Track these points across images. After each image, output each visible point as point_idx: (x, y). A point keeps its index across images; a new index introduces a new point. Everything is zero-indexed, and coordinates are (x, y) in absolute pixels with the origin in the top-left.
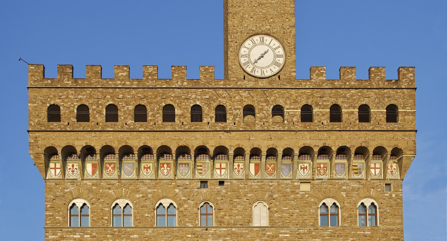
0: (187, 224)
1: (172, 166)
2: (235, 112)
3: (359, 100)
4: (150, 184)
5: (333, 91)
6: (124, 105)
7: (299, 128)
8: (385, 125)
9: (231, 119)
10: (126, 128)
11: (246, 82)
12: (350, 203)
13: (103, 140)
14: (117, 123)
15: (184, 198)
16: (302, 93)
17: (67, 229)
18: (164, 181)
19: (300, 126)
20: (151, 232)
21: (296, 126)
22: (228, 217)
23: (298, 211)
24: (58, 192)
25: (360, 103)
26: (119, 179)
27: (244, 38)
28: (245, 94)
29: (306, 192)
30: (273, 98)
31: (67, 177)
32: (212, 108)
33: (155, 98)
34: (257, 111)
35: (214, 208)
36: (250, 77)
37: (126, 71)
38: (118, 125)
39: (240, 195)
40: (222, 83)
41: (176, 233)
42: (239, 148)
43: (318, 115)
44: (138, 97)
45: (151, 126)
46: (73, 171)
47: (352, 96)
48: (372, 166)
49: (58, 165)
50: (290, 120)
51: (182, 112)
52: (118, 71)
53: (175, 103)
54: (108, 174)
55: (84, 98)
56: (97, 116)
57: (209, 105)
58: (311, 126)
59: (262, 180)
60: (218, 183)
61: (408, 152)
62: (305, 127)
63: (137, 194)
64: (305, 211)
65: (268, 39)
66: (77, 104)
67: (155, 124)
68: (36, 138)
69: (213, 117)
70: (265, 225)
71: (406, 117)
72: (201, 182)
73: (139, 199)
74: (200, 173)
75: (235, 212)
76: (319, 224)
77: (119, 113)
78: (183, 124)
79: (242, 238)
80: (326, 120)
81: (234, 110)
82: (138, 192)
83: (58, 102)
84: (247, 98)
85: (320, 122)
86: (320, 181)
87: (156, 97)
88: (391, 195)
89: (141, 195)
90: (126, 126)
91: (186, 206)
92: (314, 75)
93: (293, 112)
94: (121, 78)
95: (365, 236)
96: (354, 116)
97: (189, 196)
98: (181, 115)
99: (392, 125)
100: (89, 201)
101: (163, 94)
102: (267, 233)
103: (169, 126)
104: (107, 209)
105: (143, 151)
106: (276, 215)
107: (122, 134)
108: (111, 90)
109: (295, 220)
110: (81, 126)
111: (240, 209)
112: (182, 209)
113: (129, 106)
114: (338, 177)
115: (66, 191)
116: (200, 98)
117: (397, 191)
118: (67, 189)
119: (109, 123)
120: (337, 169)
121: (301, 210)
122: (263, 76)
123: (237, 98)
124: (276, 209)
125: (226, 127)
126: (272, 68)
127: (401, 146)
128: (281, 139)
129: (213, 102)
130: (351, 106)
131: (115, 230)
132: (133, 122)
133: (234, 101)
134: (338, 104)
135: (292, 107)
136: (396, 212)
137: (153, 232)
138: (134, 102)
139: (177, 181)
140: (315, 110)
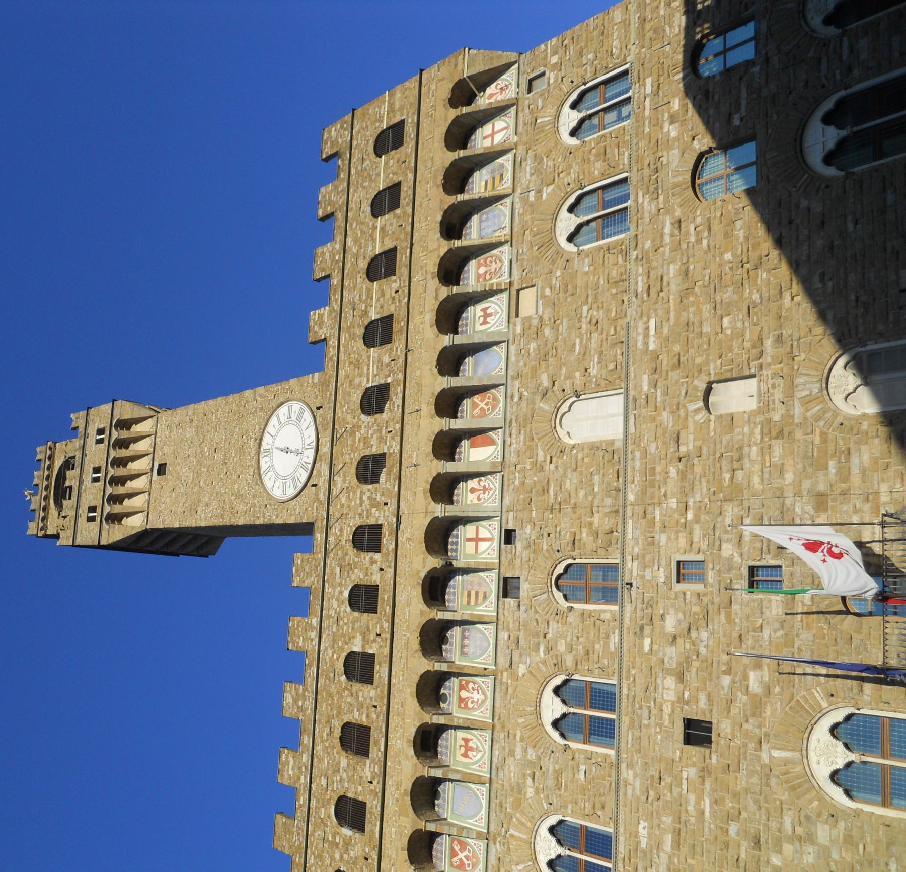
2: (367, 502)
3: (363, 223)
4: (504, 748)
5: (346, 284)
6: (338, 778)
7: (402, 346)
9: (377, 514)
10: (377, 786)
13: (397, 855)
14: (368, 806)
15: (542, 649)
18: (497, 704)
19: (398, 344)
20: (631, 773)
21: (399, 353)
22: (596, 515)
23: (585, 308)
26: (487, 837)
28: (338, 479)
30: (349, 418)
32: (357, 560)
33: (333, 699)
34: (367, 452)
35: (570, 561)
36: (315, 472)
37: (287, 757)
38: (373, 805)
39: (539, 481)
41: (638, 689)
42: (431, 491)
43: (382, 307)
44: (327, 740)
45: (378, 717)
47: (356, 241)
50: (386, 371)
51: (358, 633)
56: (352, 854)
57: (351, 567)
58: (401, 317)
60: (509, 546)
62: (400, 331)
63: (526, 793)
64: (587, 288)
65: (267, 439)
67: (375, 707)
69: (371, 558)
72: (505, 595)
73: (537, 788)
74: (485, 597)
76: (622, 236)
77: (350, 795)
78: (379, 635)
79: (658, 469)
80: (394, 283)
82: (519, 789)
84: (347, 478)
85: (393, 298)
87: (330, 695)
89: (529, 781)
90: (375, 782)
94: (296, 771)
96: (388, 223)
97: (537, 635)
98: (364, 639)
102: (645, 388)
103: (380, 671)
105: (429, 750)
106: (593, 371)
107: (389, 801)
108: (313, 803)
111: (575, 481)
113: (342, 765)
116: (339, 589)
119: (368, 828)
120: (490, 230)
121: (583, 299)
129: (347, 558)
130: (371, 235)
132: (368, 762)
133: (349, 507)
134: (366, 266)
135: (366, 371)
137: (630, 766)
138: (335, 751)
139: (500, 667)
140: (374, 315)
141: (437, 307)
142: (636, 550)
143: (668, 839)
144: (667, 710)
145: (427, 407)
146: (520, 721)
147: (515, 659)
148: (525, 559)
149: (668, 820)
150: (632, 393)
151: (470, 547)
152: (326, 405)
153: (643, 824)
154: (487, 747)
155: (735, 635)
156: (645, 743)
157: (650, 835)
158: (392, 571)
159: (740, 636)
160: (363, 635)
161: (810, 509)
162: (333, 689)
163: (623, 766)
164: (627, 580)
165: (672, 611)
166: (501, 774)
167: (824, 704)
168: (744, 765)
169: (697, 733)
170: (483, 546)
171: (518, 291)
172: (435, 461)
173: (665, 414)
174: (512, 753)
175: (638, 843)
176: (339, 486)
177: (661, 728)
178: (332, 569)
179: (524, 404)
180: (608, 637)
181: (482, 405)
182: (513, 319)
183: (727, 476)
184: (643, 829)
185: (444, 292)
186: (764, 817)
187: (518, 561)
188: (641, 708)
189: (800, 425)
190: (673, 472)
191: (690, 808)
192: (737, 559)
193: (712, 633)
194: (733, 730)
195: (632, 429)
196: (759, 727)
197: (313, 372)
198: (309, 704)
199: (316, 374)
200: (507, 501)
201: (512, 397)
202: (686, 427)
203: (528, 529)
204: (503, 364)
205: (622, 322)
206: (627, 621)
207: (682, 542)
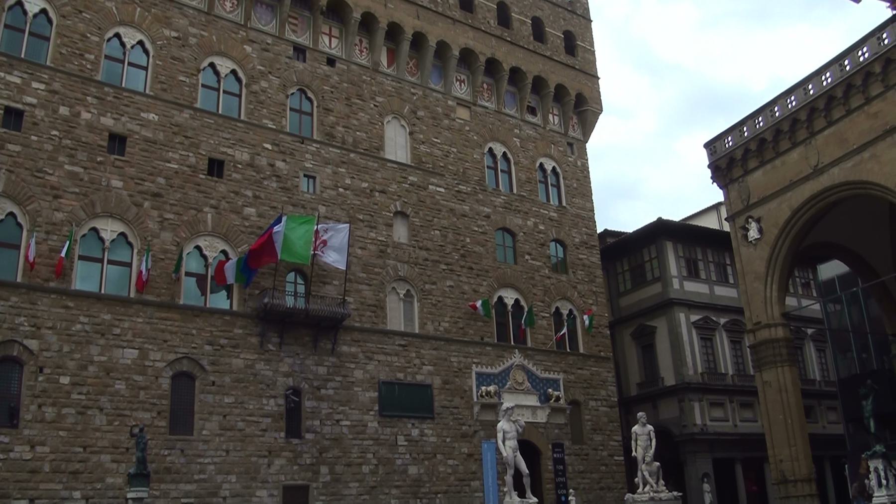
0: (265, 121)
20: (188, 116)
23: (455, 150)
43: (482, 8)
70: (404, 161)
75: (355, 122)
82: (169, 25)
89: (174, 34)
95: (551, 219)
106: (422, 147)
112: (255, 87)
124: (422, 136)
141: (477, 52)
142: (323, 152)
143: (149, 135)
144: (229, 151)
146: (214, 37)
147: (255, 45)
148: (319, 71)
149: (161, 136)
150: (409, 169)
153: (156, 118)
155: (275, 204)
157: (150, 121)
159: (275, 207)
163: (192, 112)
164: (305, 142)
165: (287, 167)
166: (176, 10)
167: (239, 250)
168: (201, 195)
169: (216, 167)
170: (326, 39)
171: (469, 108)
173: (396, 187)
174: (192, 24)
175: (143, 111)
177: (218, 144)
179: (409, 95)
180: (272, 120)
181: (411, 64)
182: (456, 101)
183: (361, 217)
184: (152, 116)
186: (172, 202)
187: (317, 65)
188: (229, 133)
189: (384, 262)
190: (365, 185)
193: (275, 190)
194: (221, 192)
195: (389, 164)
196: (224, 210)
200: (354, 67)
201: (413, 88)
206: (281, 136)
207: (327, 183)
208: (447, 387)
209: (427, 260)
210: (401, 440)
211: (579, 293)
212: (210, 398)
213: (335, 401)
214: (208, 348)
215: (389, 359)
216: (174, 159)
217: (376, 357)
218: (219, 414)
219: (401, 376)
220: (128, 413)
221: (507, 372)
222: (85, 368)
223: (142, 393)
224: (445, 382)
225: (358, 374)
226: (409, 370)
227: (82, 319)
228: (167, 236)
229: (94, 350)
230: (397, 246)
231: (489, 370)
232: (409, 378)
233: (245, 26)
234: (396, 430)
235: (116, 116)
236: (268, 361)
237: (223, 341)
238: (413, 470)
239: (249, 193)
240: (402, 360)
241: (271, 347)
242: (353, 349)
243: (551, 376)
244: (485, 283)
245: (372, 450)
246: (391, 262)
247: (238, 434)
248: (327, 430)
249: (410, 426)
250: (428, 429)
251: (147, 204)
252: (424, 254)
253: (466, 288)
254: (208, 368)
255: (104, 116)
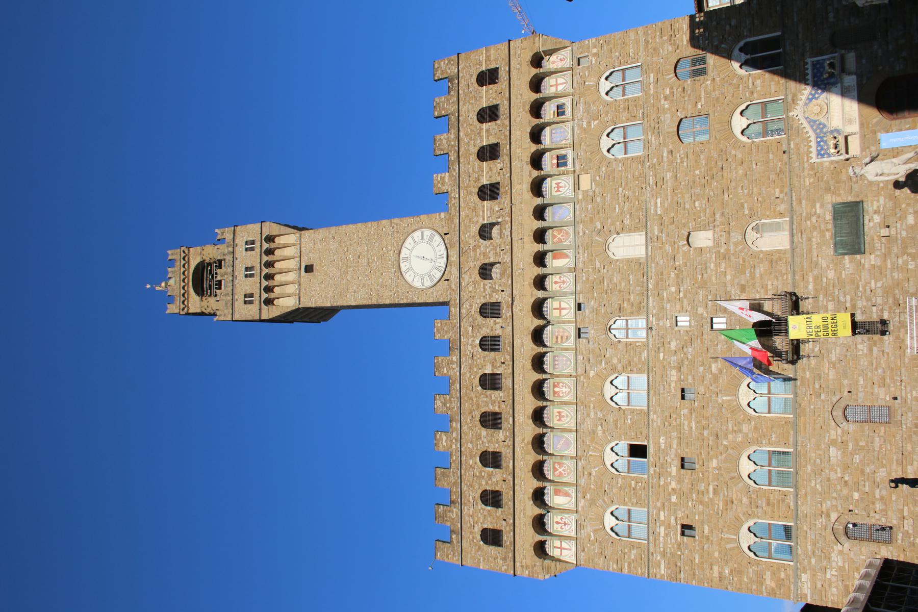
1: (557, 380)
2: (488, 291)
5: (461, 160)
8: (502, 84)
11: (452, 278)
12: (607, 112)
16: (464, 202)
17: (651, 545)
19: (504, 200)
23: (620, 189)
24: (594, 549)
25: (476, 122)
27: (404, 282)
28: (466, 279)
29: (593, 180)
30: (471, 241)
31: (573, 534)
34: (487, 261)
38: (506, 452)
40: (453, 309)
46: (565, 524)
47: (467, 135)
48: (553, 90)
49: (557, 543)
50: (497, 215)
51: (489, 363)
52: (440, 445)
53: (477, 373)
54: (568, 474)
55: (472, 495)
57: (480, 327)
59: (576, 247)
61: (537, 45)
62: (506, 192)
66: (481, 505)
68: (522, 567)
70: (644, 237)
71: (492, 58)
75: (623, 284)
77: (491, 450)
80: (497, 164)
81: (485, 292)
82: (594, 432)
83: (477, 530)
86: (576, 162)
87: (471, 399)
88: (594, 55)
89: (600, 428)
91: (615, 361)
92: (444, 188)
93: (487, 211)
99: (503, 74)
100: (608, 507)
101: (468, 389)
103: (506, 382)
104: (620, 480)
106: (627, 222)
107: (517, 449)
108: (464, 458)
109: (634, 192)
110: (507, 504)
112: (619, 367)
114: (570, 136)
115: (592, 538)
117: (589, 48)
118: (590, 536)
119: (504, 465)
122: (445, 256)
123: (471, 289)
125: (507, 302)
126: (435, 244)
127: (528, 56)
128: (521, 224)
131: (652, 472)
136: (619, 42)
137: (655, 413)
140: (485, 181)
143: (675, 442)
144: (673, 385)
145: (529, 238)
149: (674, 434)
150: (649, 235)
151: (556, 313)
152: (452, 233)
154: (573, 414)
155: (705, 349)
156: (662, 401)
158: (510, 328)
160: (492, 364)
161: (738, 291)
162: (472, 395)
166: (582, 426)
168: (710, 405)
170: (564, 312)
172: (536, 267)
174: (588, 415)
175: (660, 447)
176: (467, 280)
178: (466, 329)
181: (559, 236)
184: (662, 440)
185: (535, 173)
187: (587, 319)
190: (672, 275)
191: (686, 427)
192: (705, 315)
195: (650, 253)
197: (440, 212)
198: (455, 405)
199: (442, 214)
200: (578, 288)
202: (678, 253)
203: (592, 303)
204: (572, 215)
205: (643, 198)
206: (651, 346)
207: (678, 307)
208: (832, 188)
209: (723, 214)
210: (885, 232)
211: (722, 43)
212: (861, 395)
213: (856, 294)
214: (823, 397)
215: (815, 246)
216: (689, 424)
217: (815, 259)
218: (873, 388)
219: (828, 235)
220: (876, 453)
221: (812, 123)
222: (846, 482)
223: (861, 443)
224: (828, 190)
225: (831, 274)
226: (822, 227)
227: (813, 485)
228: (745, 428)
229: (833, 476)
230: (717, 244)
231: (813, 144)
232: (830, 226)
233: (576, 377)
234: (875, 238)
235: (668, 465)
236: (829, 351)
237: (817, 386)
238: (911, 220)
239: (701, 369)
240: (815, 234)
241: (817, 349)
242: (811, 280)
243: (809, 71)
244: (733, 152)
245: (895, 260)
246: (732, 248)
247: (888, 373)
248: (880, 301)
249: (871, 224)
250: (870, 207)
251: (725, 443)
252: (718, 216)
253: (741, 172)
254: (838, 397)
255: (670, 473)
